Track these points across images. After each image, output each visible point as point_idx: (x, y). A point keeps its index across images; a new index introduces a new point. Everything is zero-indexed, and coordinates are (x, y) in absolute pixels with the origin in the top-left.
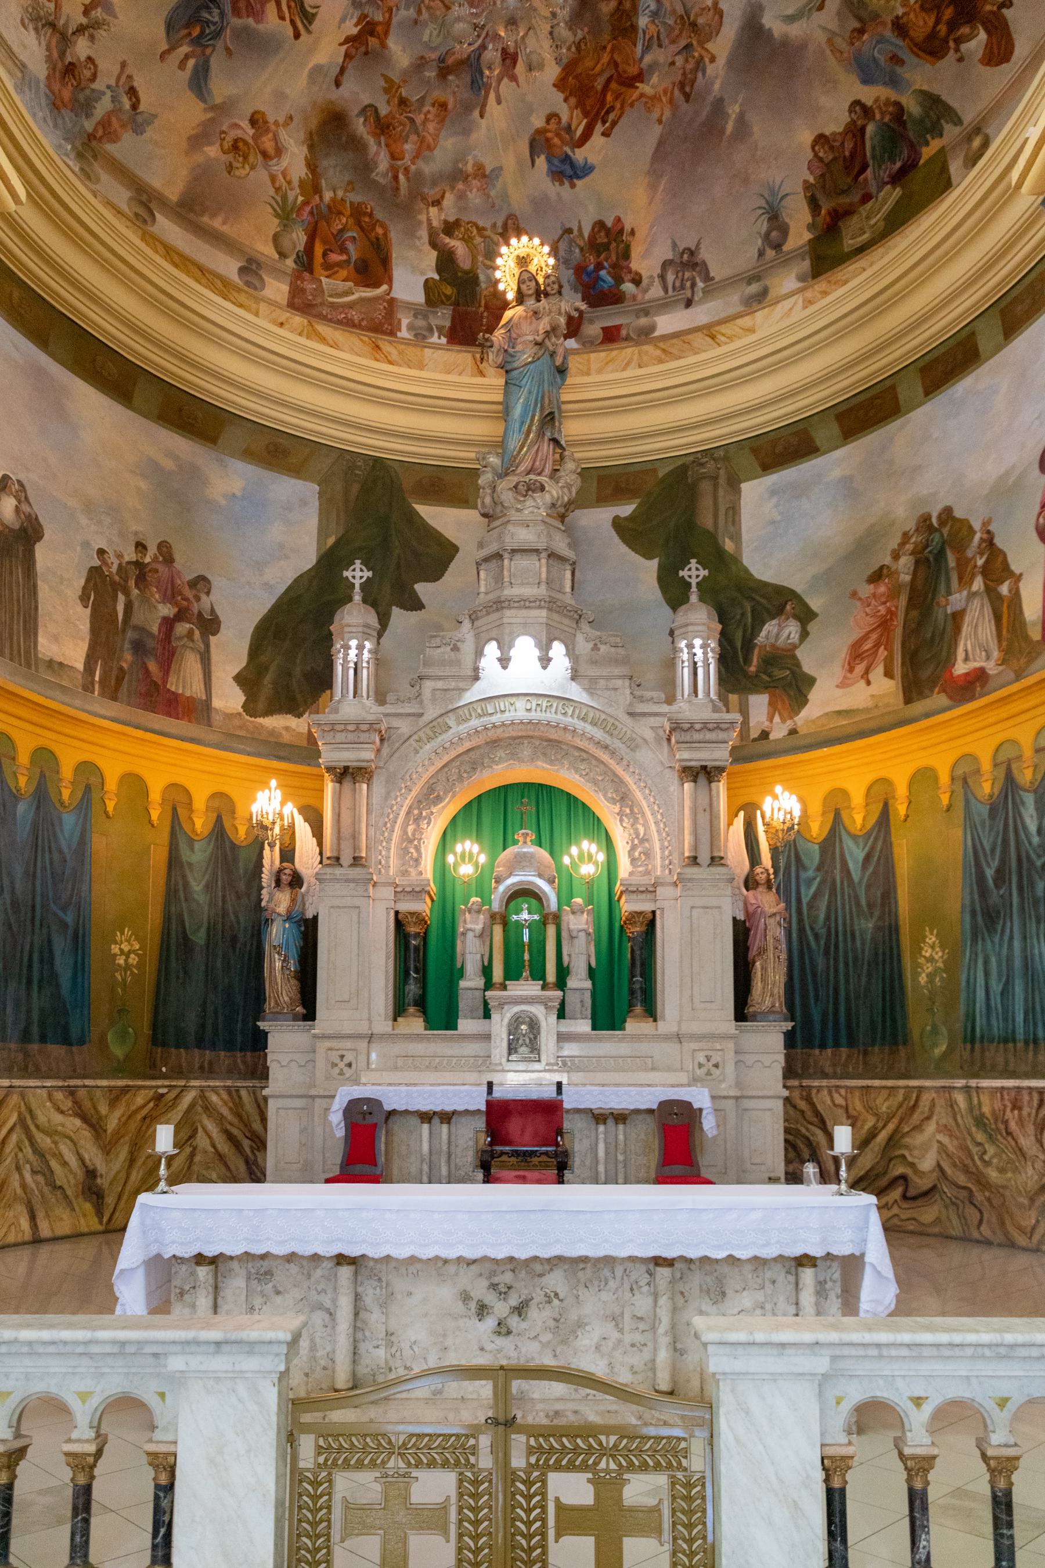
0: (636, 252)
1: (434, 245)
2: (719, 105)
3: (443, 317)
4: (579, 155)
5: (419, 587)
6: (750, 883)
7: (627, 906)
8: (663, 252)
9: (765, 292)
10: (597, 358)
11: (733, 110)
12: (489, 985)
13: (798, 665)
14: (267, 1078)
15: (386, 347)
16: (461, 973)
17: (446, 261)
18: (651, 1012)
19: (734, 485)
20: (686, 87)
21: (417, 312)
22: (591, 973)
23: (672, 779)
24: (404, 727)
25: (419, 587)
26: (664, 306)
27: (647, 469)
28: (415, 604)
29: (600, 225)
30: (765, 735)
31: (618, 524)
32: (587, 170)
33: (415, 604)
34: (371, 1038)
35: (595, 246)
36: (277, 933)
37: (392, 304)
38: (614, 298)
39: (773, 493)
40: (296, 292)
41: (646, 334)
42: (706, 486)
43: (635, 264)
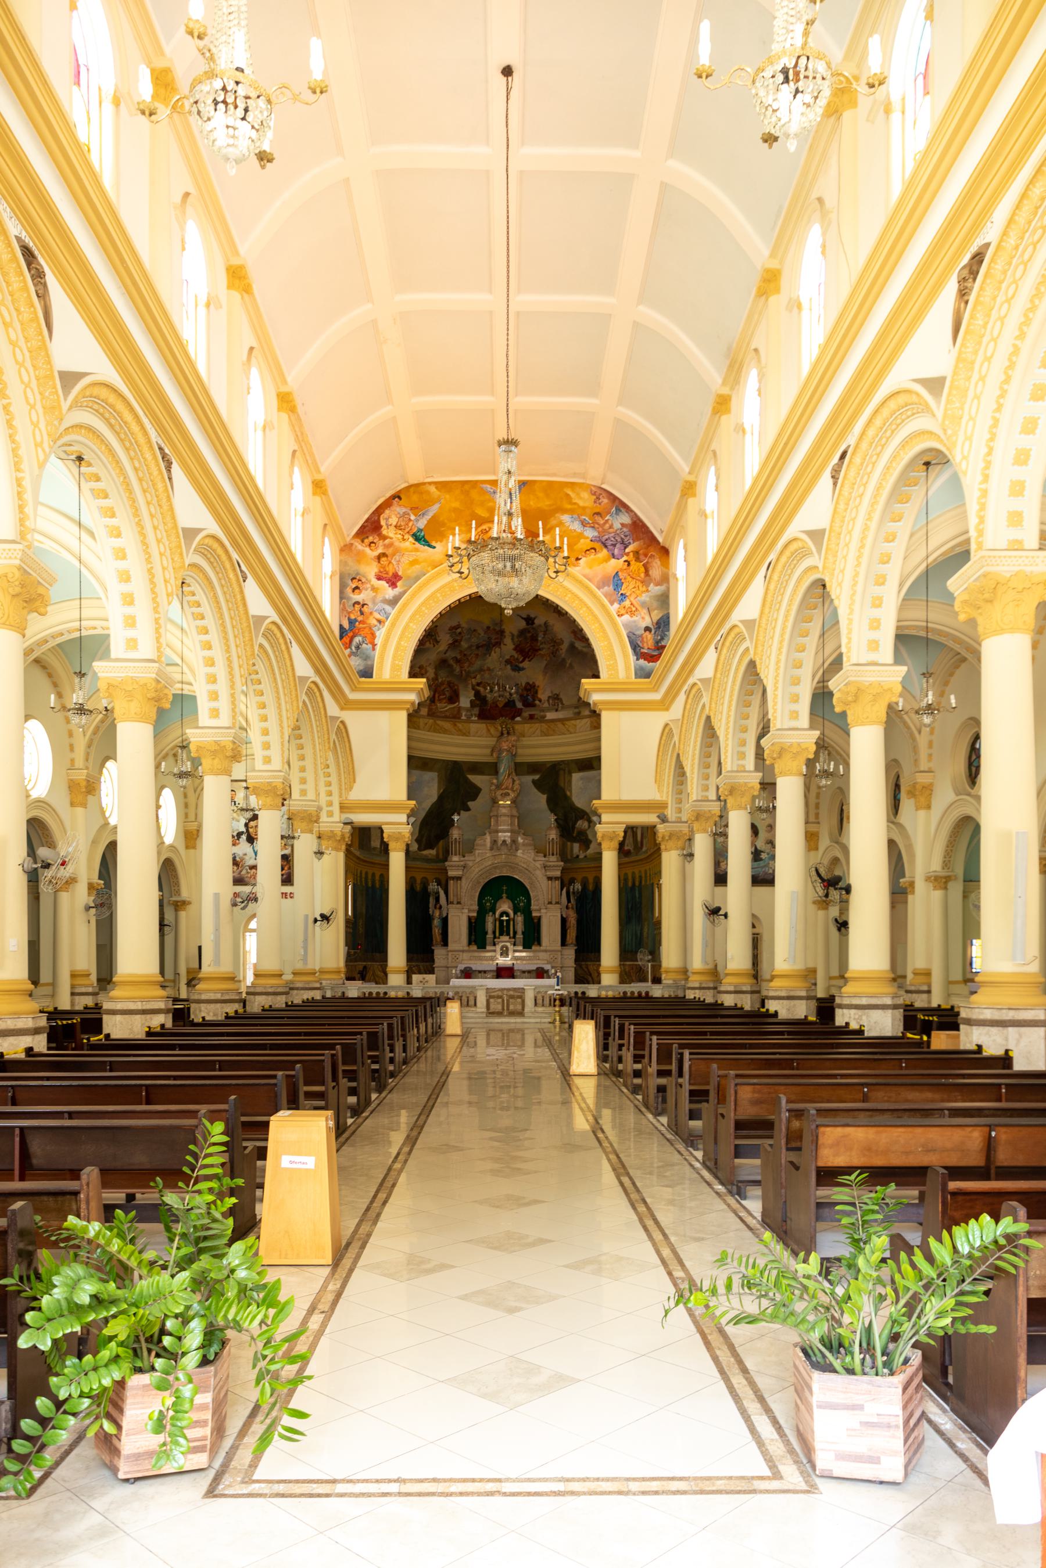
0: (540, 692)
1: (473, 689)
2: (564, 660)
3: (476, 711)
4: (521, 665)
5: (470, 804)
6: (567, 907)
7: (534, 914)
8: (548, 693)
9: (579, 713)
10: (527, 726)
11: (569, 662)
12: (495, 937)
13: (587, 835)
14: (433, 961)
15: (460, 725)
16: (486, 933)
17: (477, 694)
18: (539, 944)
19: (570, 773)
20: (554, 654)
21: (467, 710)
22: (523, 933)
23: (545, 878)
24: (470, 864)
25: (470, 804)
26: (549, 710)
27: (544, 764)
28: (468, 809)
29: (528, 683)
30: (578, 856)
31: (534, 782)
32: (523, 669)
33: (468, 809)
34: (463, 951)
35: (526, 689)
36: (436, 922)
37: (459, 709)
38: (533, 705)
39: (582, 779)
40: (430, 710)
41: (542, 719)
42: (561, 772)
43: (540, 695)
